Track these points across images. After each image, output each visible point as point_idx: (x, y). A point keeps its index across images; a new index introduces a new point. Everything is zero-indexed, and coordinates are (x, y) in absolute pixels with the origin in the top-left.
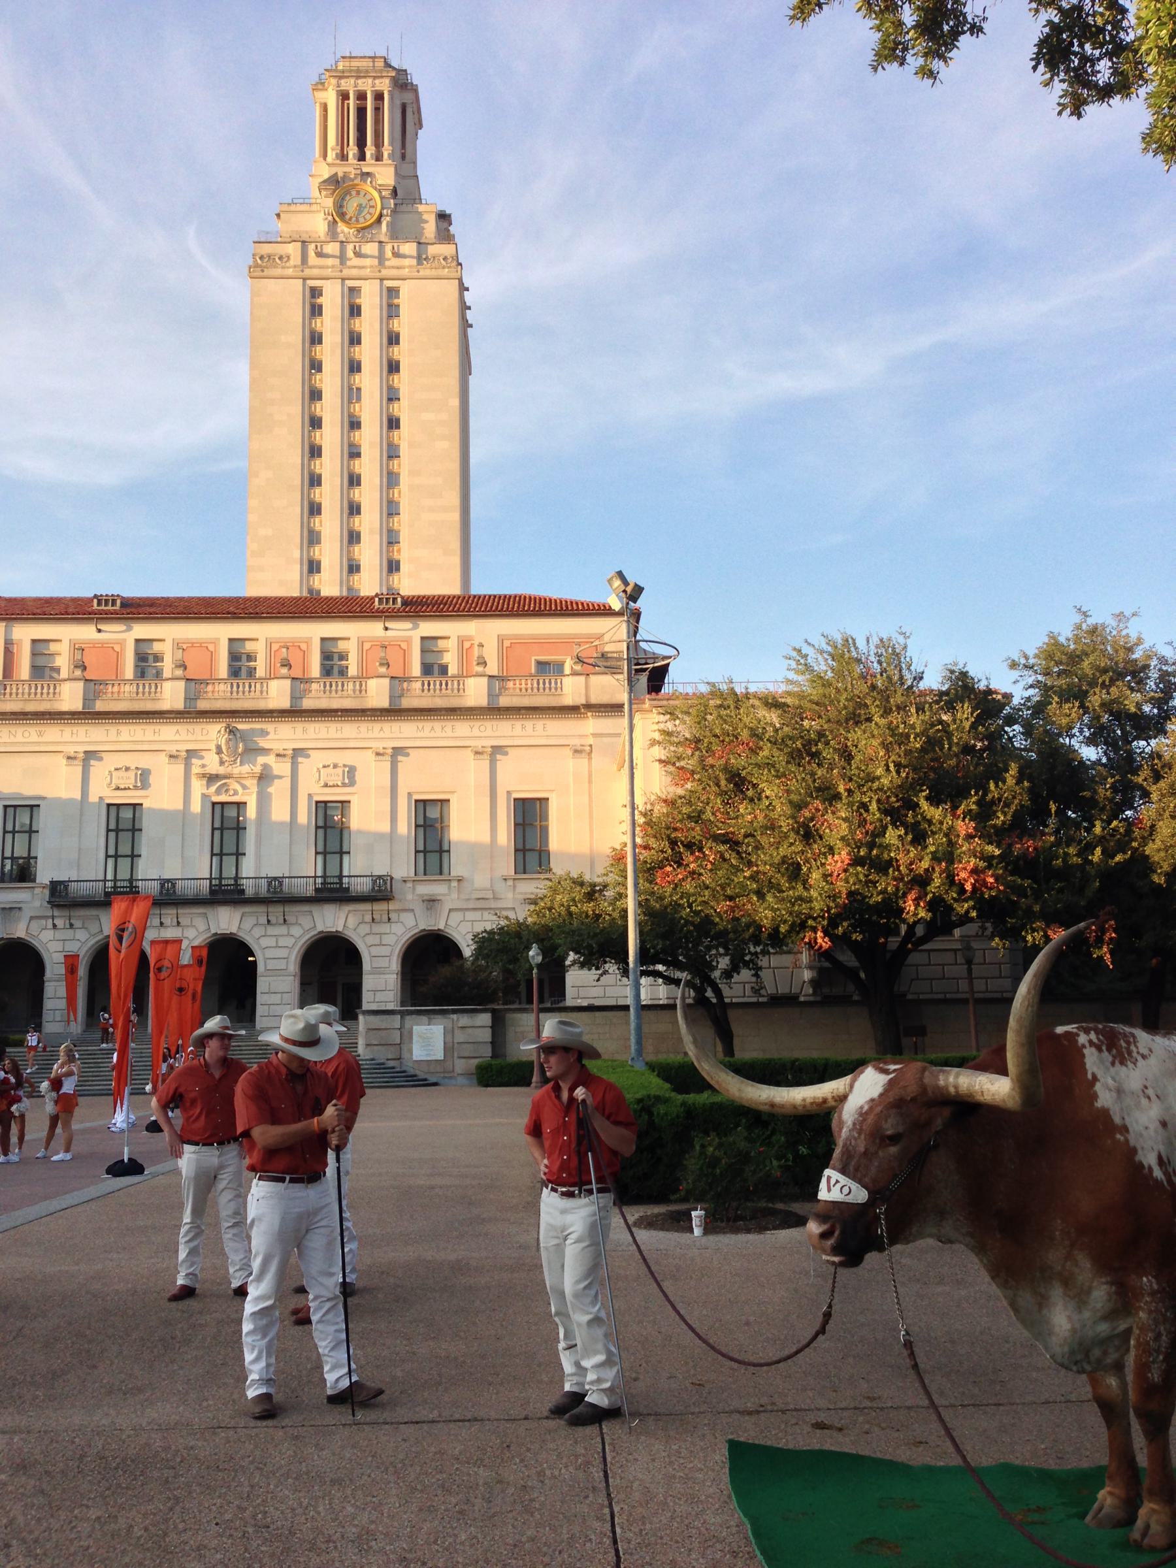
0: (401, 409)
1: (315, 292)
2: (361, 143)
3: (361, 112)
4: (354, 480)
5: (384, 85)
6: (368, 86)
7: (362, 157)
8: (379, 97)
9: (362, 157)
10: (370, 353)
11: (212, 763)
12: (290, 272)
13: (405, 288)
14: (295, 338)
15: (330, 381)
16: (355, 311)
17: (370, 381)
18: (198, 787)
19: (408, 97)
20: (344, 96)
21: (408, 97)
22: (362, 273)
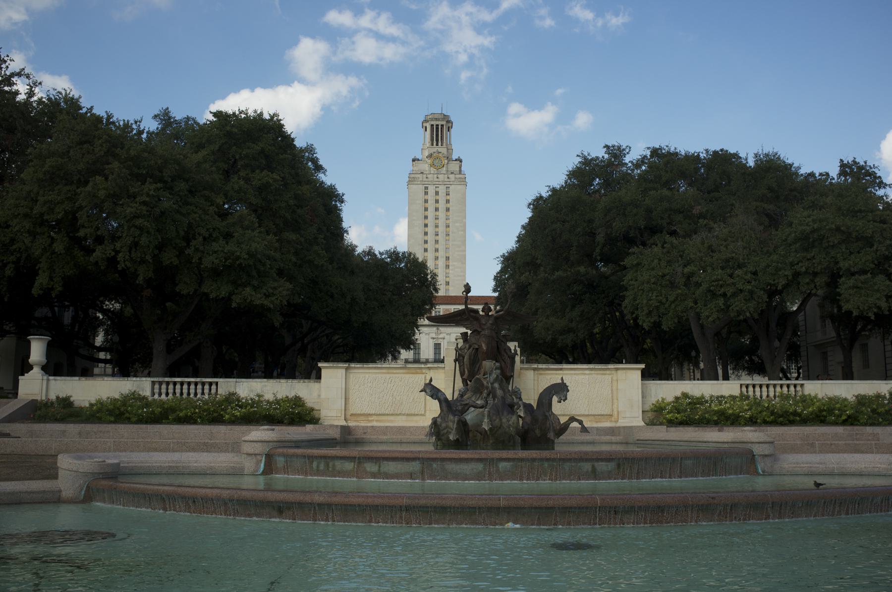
0: (450, 222)
1: (426, 188)
2: (437, 140)
3: (437, 128)
4: (437, 242)
5: (444, 123)
6: (440, 123)
7: (437, 145)
8: (442, 126)
9: (437, 145)
10: (442, 205)
11: (434, 335)
12: (419, 183)
13: (452, 187)
14: (420, 202)
15: (431, 213)
16: (437, 193)
17: (442, 214)
18: (431, 341)
19: (450, 125)
20: (432, 125)
21: (450, 125)
22: (440, 183)
